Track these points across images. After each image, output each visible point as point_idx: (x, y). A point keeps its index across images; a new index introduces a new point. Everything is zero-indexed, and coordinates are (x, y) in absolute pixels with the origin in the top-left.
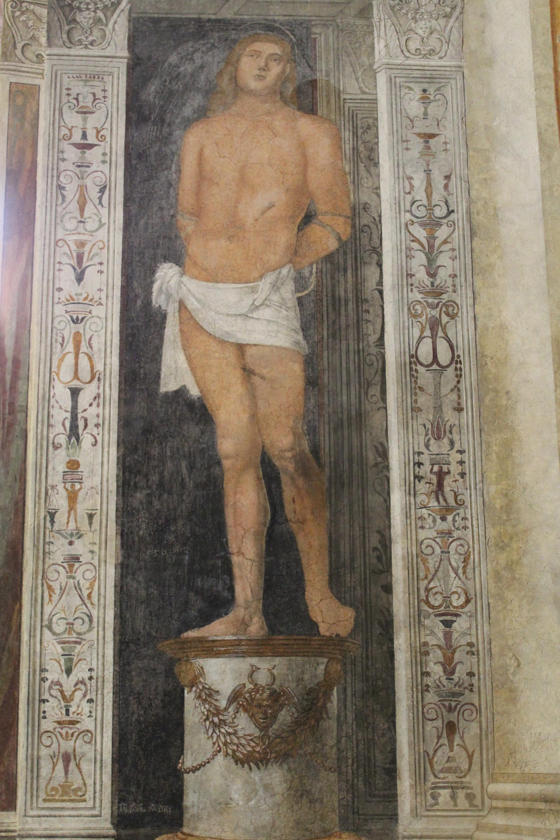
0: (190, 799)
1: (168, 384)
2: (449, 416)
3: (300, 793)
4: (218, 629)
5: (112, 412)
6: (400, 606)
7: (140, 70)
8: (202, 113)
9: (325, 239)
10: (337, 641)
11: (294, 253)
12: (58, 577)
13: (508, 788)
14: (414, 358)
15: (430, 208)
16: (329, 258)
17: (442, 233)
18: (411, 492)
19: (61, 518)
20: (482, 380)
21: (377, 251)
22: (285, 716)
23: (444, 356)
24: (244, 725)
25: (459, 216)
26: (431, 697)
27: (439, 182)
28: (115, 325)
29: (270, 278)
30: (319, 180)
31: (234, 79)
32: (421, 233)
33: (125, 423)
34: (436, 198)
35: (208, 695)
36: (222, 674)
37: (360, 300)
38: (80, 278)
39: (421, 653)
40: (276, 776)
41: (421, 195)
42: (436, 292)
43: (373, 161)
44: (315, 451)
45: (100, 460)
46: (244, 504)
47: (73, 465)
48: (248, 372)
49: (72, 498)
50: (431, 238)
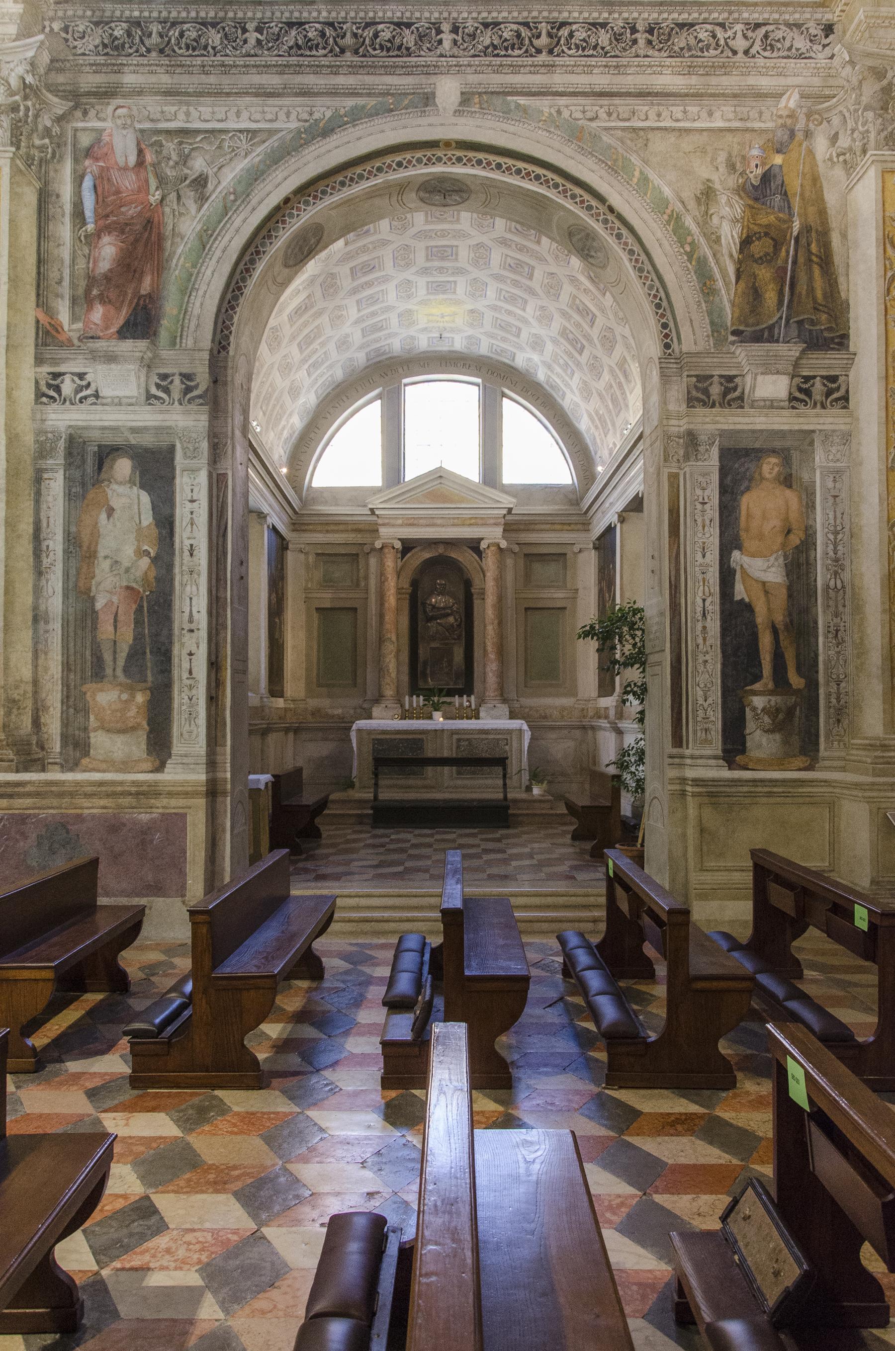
0: (748, 744)
1: (737, 598)
2: (841, 609)
3: (786, 742)
4: (757, 686)
5: (717, 608)
6: (821, 679)
7: (724, 472)
8: (748, 489)
9: (795, 540)
10: (799, 690)
11: (783, 545)
12: (701, 668)
13: (859, 742)
14: (828, 586)
15: (835, 526)
16: (797, 547)
17: (840, 537)
18: (826, 637)
19: (701, 647)
20: (854, 594)
21: (815, 544)
22: (781, 716)
23: (839, 586)
24: (767, 719)
25: (847, 530)
26: (832, 710)
27: (839, 515)
28: (717, 575)
29: (774, 556)
30: (794, 515)
31: (760, 474)
32: (831, 537)
33: (722, 612)
34: (838, 522)
35: (754, 709)
36: (759, 702)
37: (808, 563)
38: (704, 556)
39: (828, 695)
40: (777, 736)
41: (832, 522)
42: (837, 560)
43: (814, 507)
44: (791, 621)
45: (714, 625)
46: (766, 641)
47: (704, 628)
48: (766, 592)
49: (705, 639)
50: (836, 538)
